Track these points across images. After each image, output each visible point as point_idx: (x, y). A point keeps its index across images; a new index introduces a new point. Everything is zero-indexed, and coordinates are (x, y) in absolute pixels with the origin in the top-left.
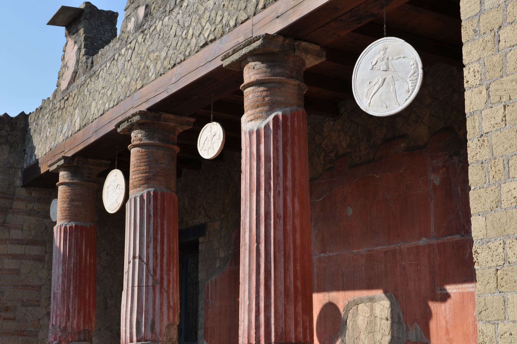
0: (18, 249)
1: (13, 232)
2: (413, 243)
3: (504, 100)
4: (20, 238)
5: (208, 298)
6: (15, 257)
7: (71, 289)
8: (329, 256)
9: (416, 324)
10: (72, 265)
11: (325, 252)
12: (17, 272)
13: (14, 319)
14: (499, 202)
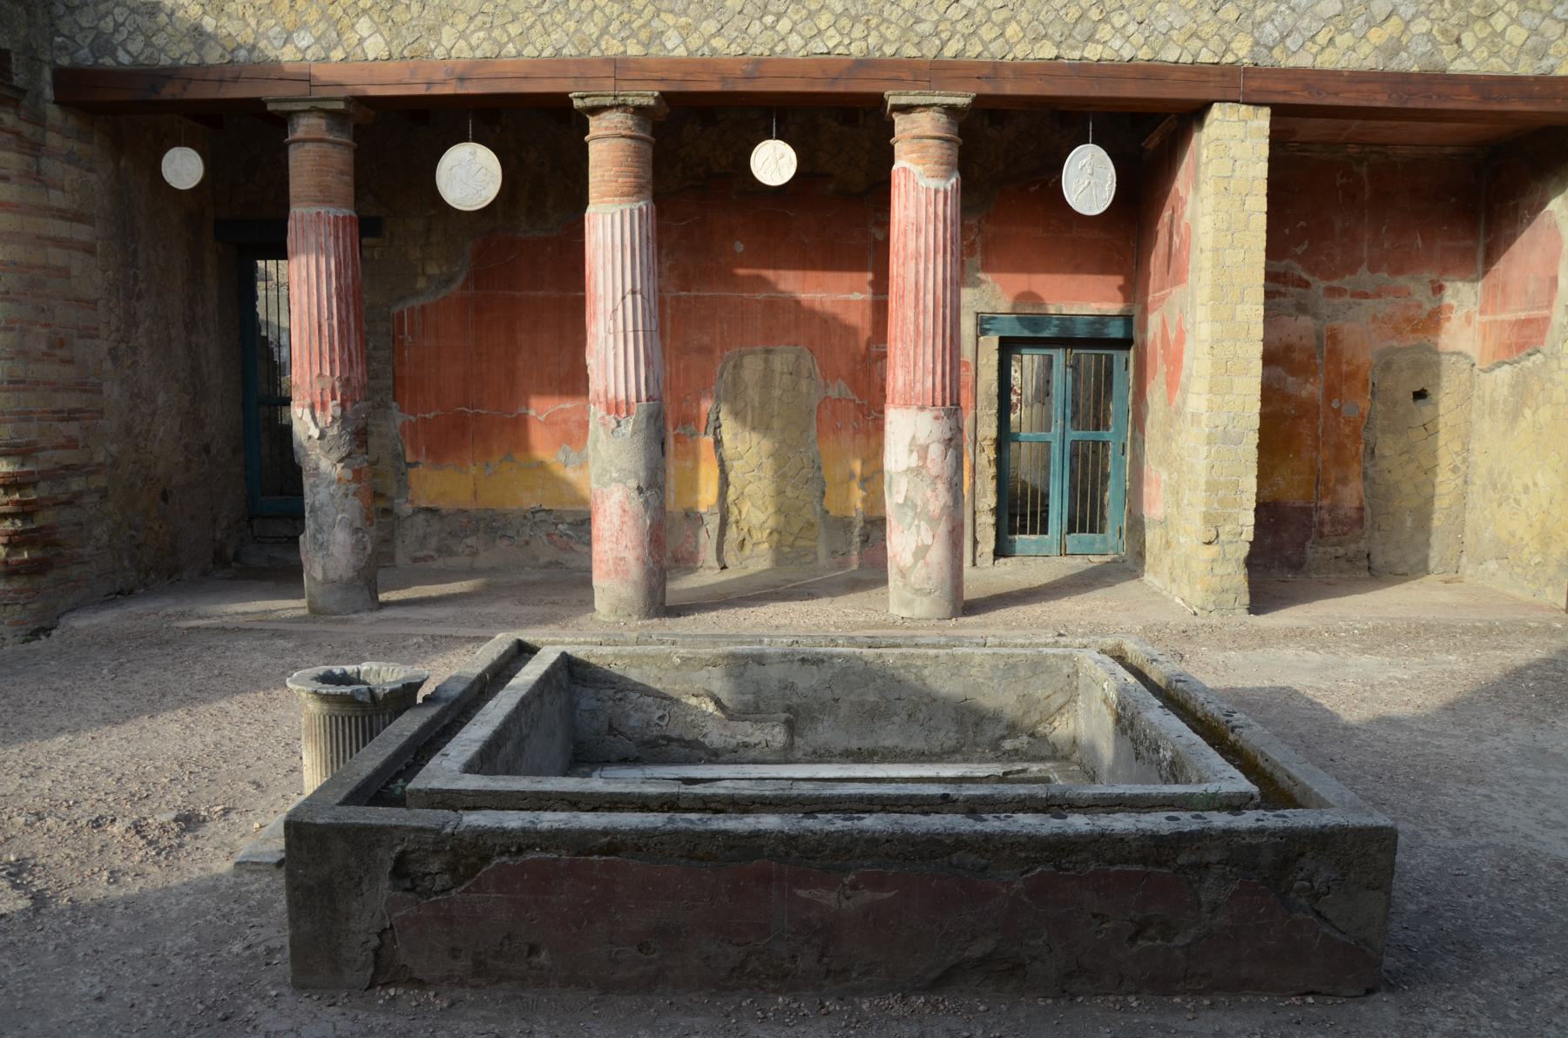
0: (61, 229)
1: (52, 192)
2: (844, 296)
3: (1246, 247)
4: (63, 206)
5: (402, 332)
6: (59, 242)
7: (352, 318)
8: (696, 297)
9: (840, 380)
10: (350, 281)
11: (689, 291)
12: (64, 272)
13: (70, 362)
14: (1233, 317)
